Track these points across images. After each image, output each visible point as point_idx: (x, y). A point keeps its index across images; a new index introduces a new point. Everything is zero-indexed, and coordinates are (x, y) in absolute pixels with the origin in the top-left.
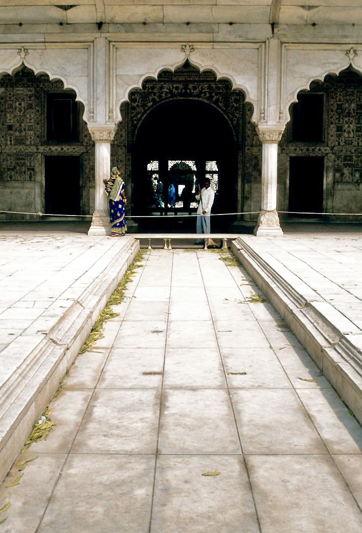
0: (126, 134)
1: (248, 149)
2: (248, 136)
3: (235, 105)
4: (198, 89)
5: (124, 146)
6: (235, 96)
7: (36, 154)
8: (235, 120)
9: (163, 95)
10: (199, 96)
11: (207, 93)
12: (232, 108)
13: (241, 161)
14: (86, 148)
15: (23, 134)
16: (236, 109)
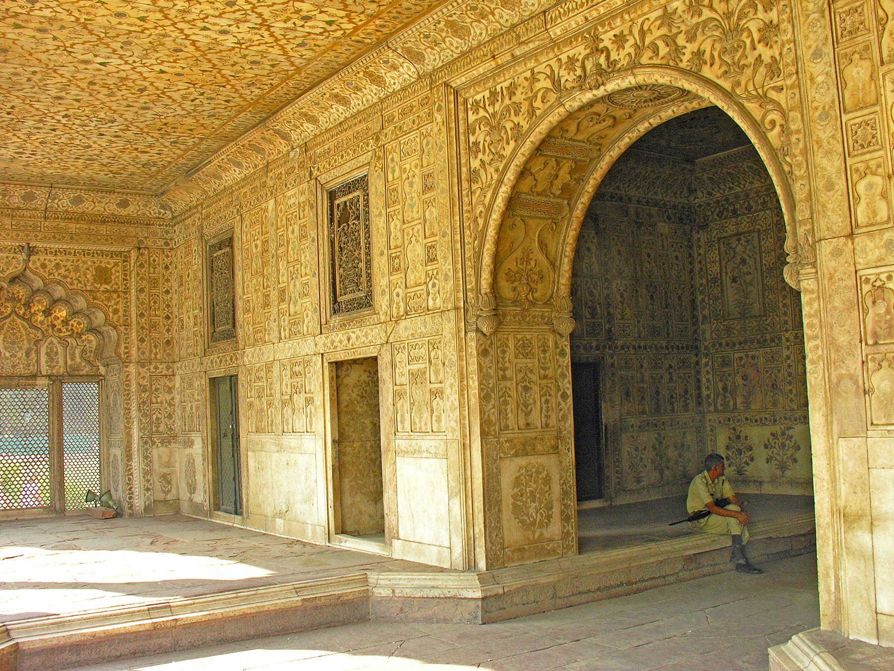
0: (455, 271)
1: (837, 253)
2: (830, 186)
3: (767, 54)
4: (631, 41)
5: (457, 308)
6: (760, 15)
7: (314, 358)
8: (773, 123)
9: (538, 104)
10: (634, 65)
11: (661, 44)
12: (755, 72)
13: (816, 321)
14: (386, 332)
15: (298, 307)
16: (774, 69)
